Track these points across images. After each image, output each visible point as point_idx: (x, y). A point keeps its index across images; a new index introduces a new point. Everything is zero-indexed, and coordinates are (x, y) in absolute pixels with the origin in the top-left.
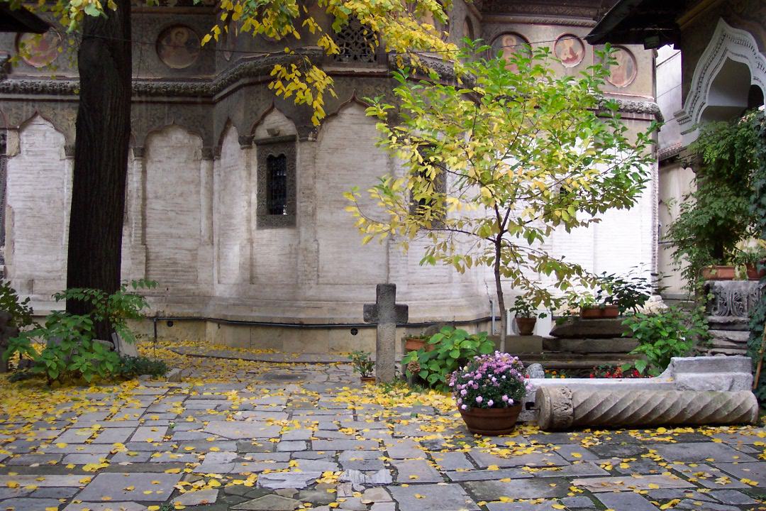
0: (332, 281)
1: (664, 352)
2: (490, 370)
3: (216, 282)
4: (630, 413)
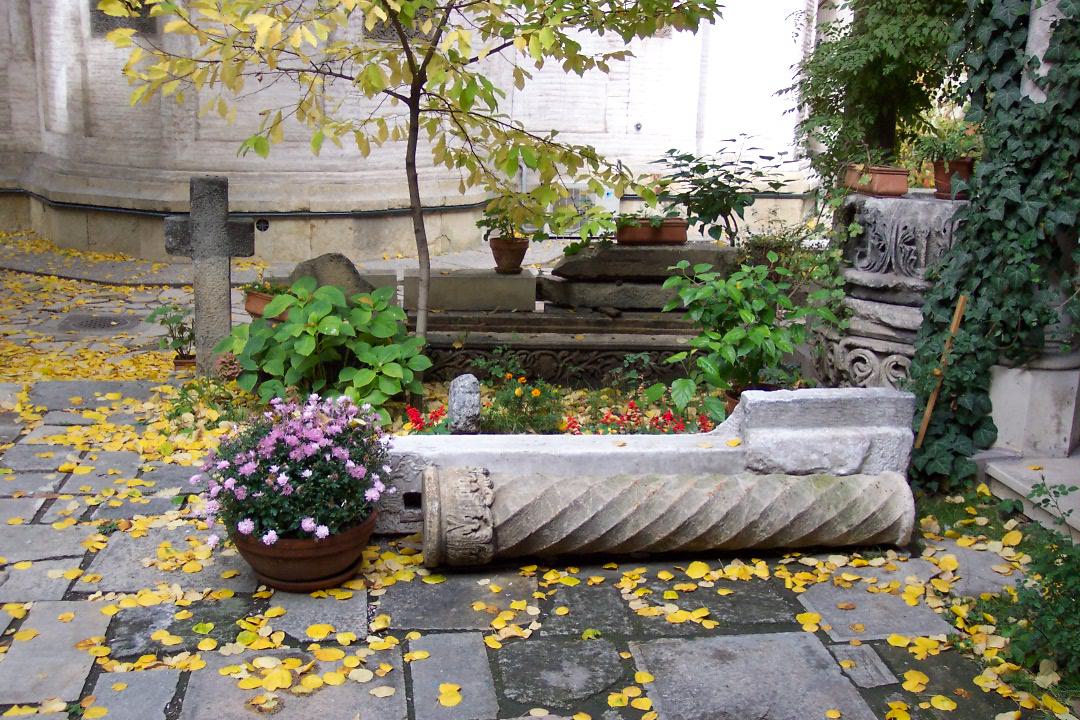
0: (222, 135)
1: (743, 353)
2: (281, 452)
3: (43, 128)
4: (629, 533)
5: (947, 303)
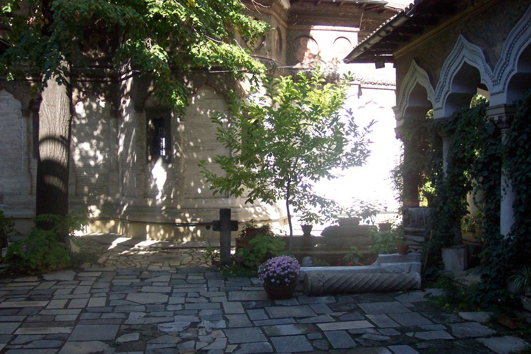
4: (354, 285)
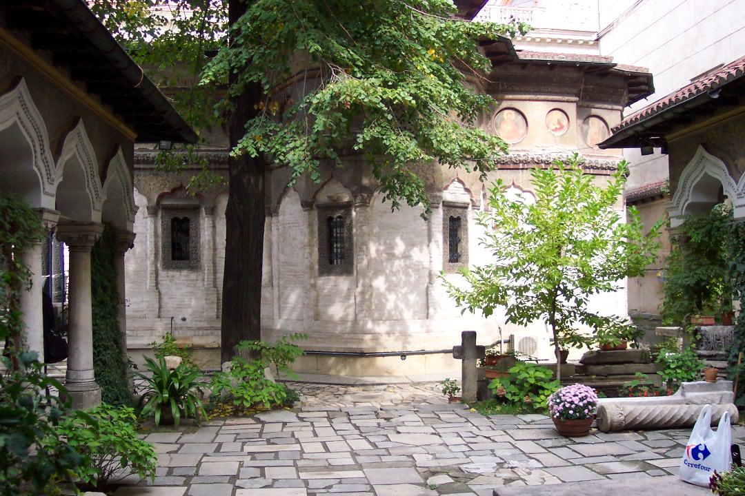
5: (736, 356)
